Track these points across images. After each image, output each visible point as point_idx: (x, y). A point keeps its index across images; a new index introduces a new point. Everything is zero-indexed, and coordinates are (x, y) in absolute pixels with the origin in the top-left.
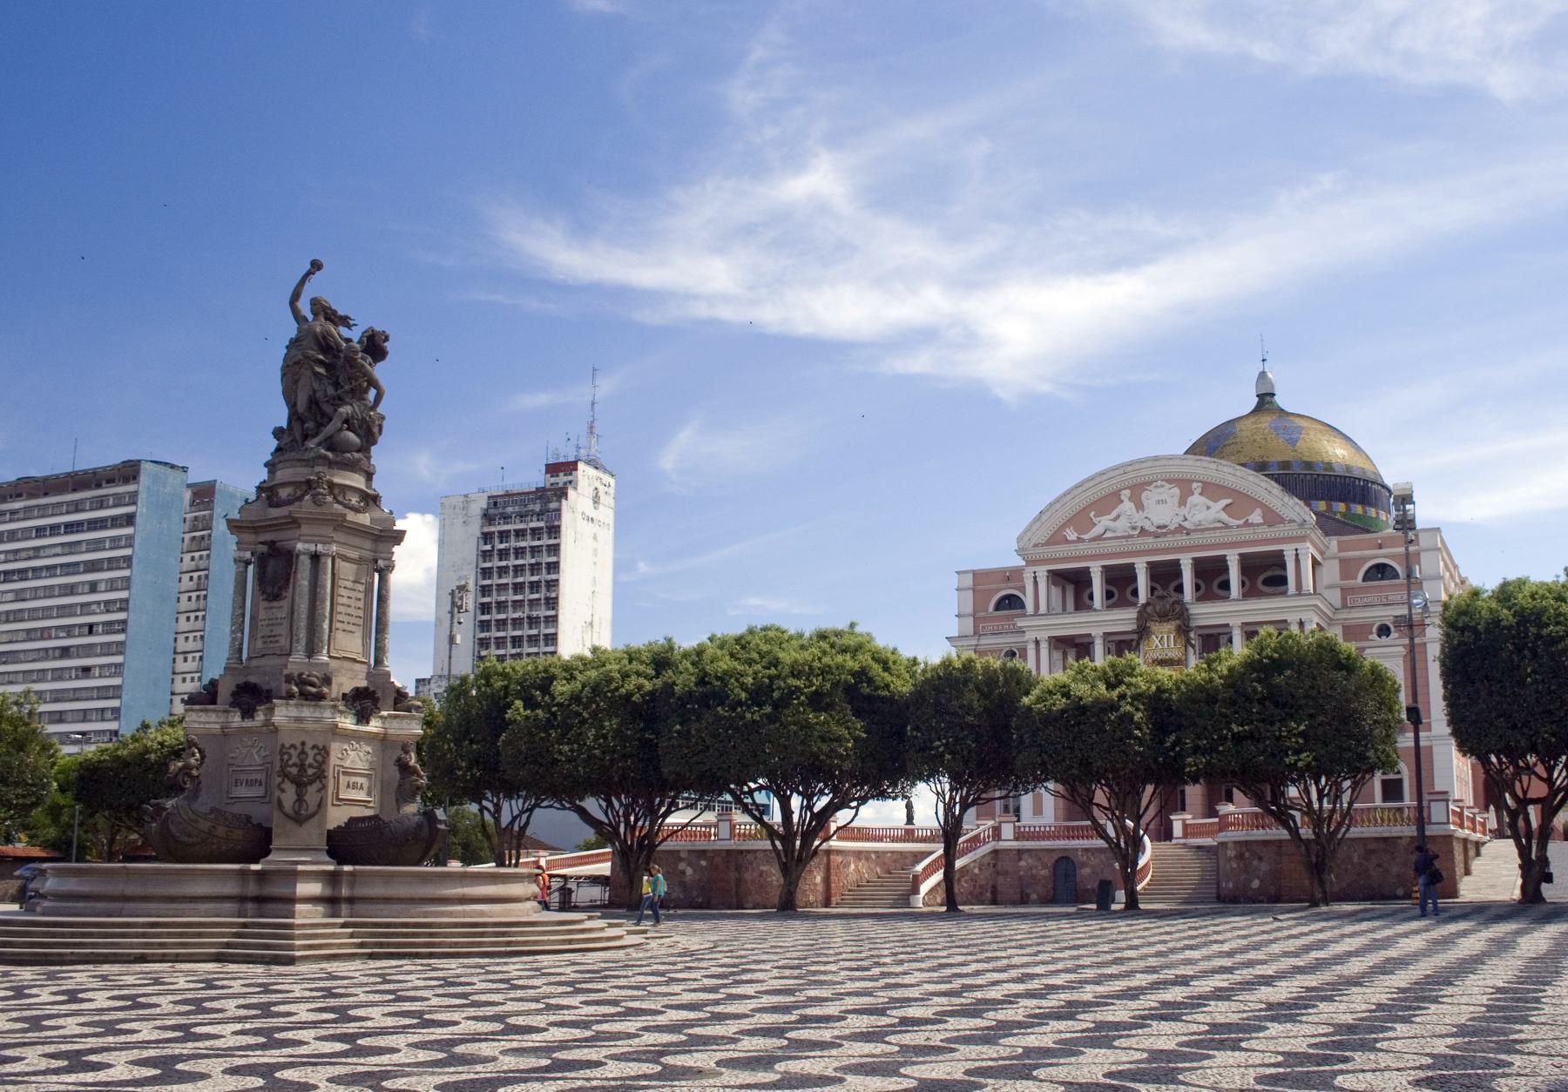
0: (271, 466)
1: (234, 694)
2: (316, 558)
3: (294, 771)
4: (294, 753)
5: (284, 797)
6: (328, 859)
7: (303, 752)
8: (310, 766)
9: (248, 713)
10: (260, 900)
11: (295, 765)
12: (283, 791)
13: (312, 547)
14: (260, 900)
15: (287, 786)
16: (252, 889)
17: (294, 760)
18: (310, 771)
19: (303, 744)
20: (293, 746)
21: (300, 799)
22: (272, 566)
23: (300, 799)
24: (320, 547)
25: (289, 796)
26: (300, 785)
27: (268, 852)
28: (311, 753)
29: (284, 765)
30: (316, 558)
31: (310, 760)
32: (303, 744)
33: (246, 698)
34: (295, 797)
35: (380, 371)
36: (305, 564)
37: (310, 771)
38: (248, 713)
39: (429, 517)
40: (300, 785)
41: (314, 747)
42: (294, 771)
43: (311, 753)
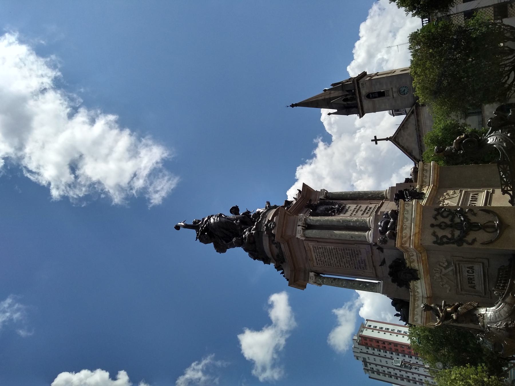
0: (267, 261)
1: (400, 285)
3: (457, 233)
4: (440, 233)
8: (452, 220)
12: (474, 240)
13: (299, 228)
15: (469, 238)
19: (432, 226)
20: (434, 234)
21: (483, 227)
23: (483, 227)
25: (482, 236)
29: (451, 241)
31: (447, 221)
32: (432, 226)
35: (159, 161)
41: (435, 218)
42: (457, 233)
43: (441, 219)
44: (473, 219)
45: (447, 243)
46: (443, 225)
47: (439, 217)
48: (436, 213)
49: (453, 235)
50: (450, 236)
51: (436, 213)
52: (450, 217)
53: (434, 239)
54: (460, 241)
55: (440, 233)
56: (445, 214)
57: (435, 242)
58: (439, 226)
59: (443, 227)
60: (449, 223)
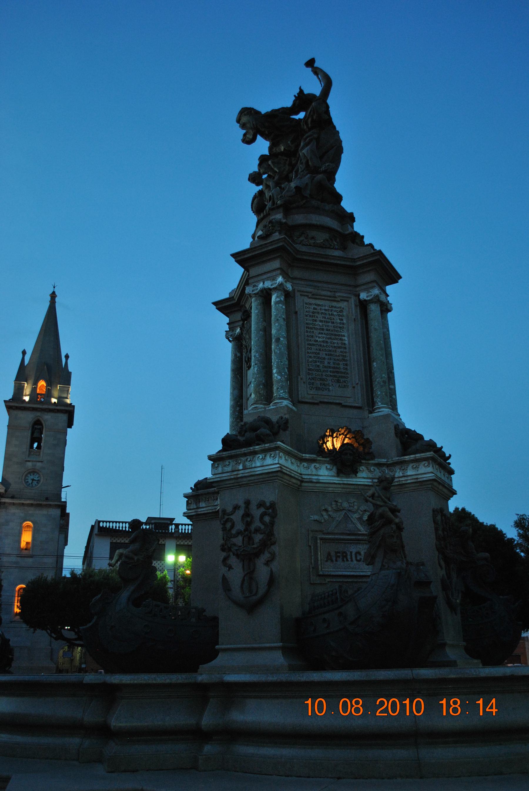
3: (238, 541)
8: (257, 530)
11: (239, 533)
12: (230, 568)
15: (233, 561)
17: (240, 526)
18: (258, 538)
19: (248, 503)
20: (236, 508)
21: (250, 575)
26: (249, 558)
27: (214, 655)
28: (257, 513)
31: (257, 524)
32: (248, 503)
40: (249, 558)
45: (224, 529)
46: (249, 519)
47: (262, 510)
50: (234, 532)
52: (262, 527)
53: (229, 509)
55: (237, 517)
58: (247, 514)
59: (249, 519)
60: (253, 527)
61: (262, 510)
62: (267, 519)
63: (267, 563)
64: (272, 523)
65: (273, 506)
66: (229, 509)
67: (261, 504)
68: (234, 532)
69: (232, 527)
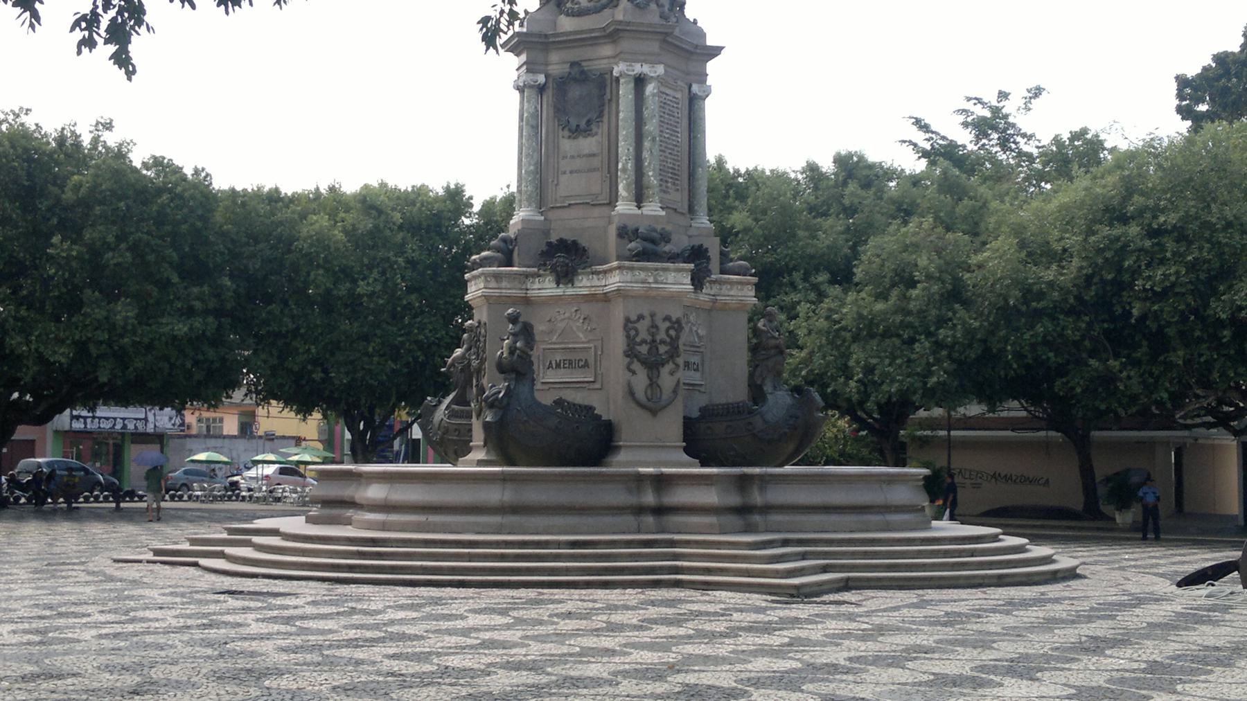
2: (640, 81)
3: (644, 349)
5: (634, 379)
6: (686, 457)
7: (654, 326)
8: (663, 342)
9: (565, 276)
10: (660, 511)
11: (644, 342)
12: (634, 373)
13: (638, 69)
14: (660, 511)
15: (636, 366)
16: (649, 498)
18: (663, 349)
19: (652, 315)
20: (641, 317)
22: (575, 92)
23: (653, 384)
24: (645, 69)
25: (641, 380)
26: (653, 366)
30: (640, 81)
31: (662, 335)
32: (652, 315)
33: (560, 258)
34: (646, 381)
36: (626, 92)
37: (663, 349)
38: (565, 276)
39: (1237, 49)
40: (653, 366)
42: (644, 349)
43: (664, 326)
44: (665, 371)
45: (628, 337)
47: (668, 324)
48: (674, 319)
49: (640, 344)
50: (638, 340)
51: (674, 319)
53: (634, 318)
54: (631, 353)
55: (643, 326)
56: (672, 333)
57: (628, 320)
58: (654, 326)
60: (658, 338)
61: (668, 324)
62: (672, 333)
63: (672, 373)
64: (678, 337)
65: (678, 322)
66: (634, 318)
67: (667, 318)
68: (638, 340)
69: (637, 334)
